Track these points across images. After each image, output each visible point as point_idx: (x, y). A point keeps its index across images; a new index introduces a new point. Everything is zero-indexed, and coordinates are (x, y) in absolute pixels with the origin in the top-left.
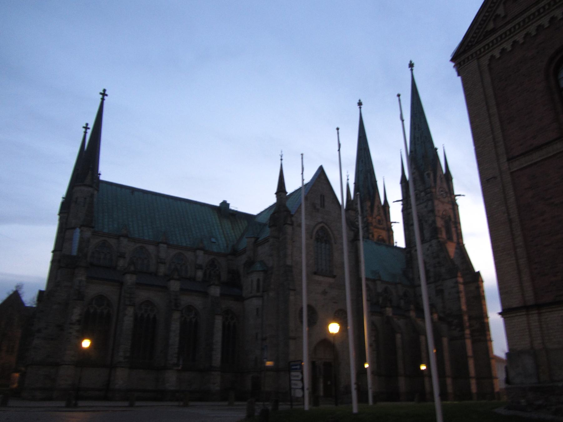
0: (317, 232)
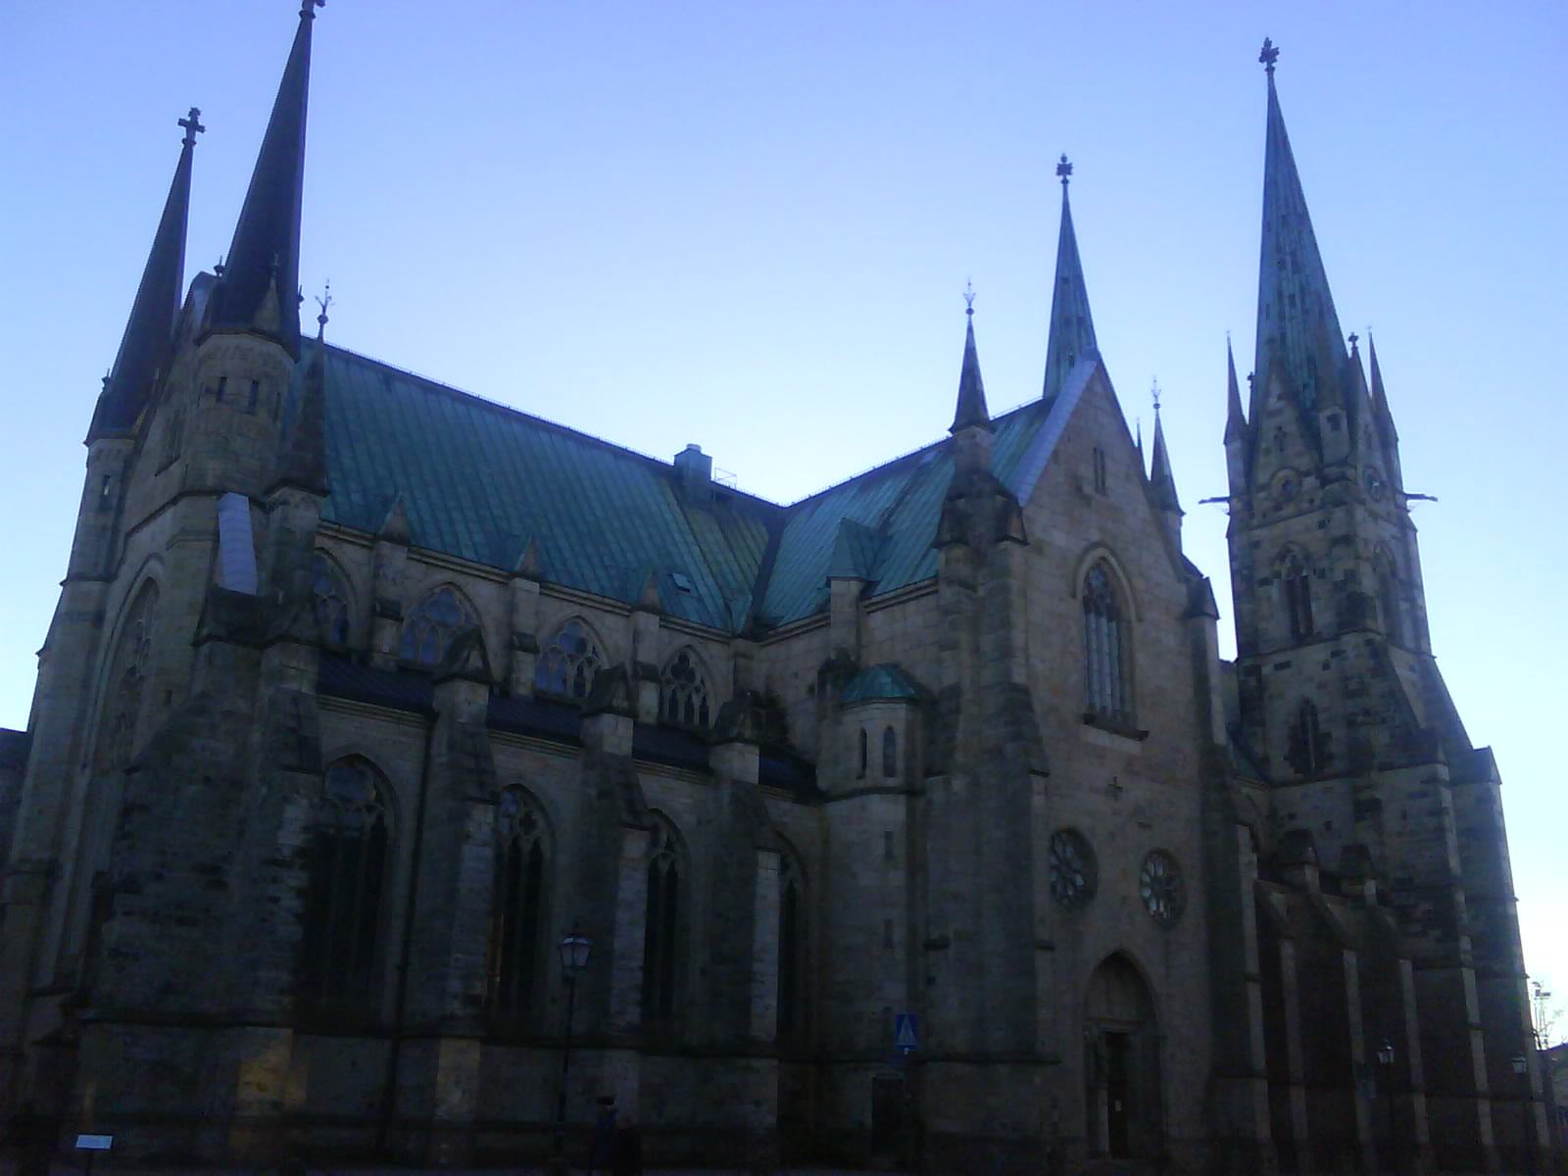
0: (1087, 578)
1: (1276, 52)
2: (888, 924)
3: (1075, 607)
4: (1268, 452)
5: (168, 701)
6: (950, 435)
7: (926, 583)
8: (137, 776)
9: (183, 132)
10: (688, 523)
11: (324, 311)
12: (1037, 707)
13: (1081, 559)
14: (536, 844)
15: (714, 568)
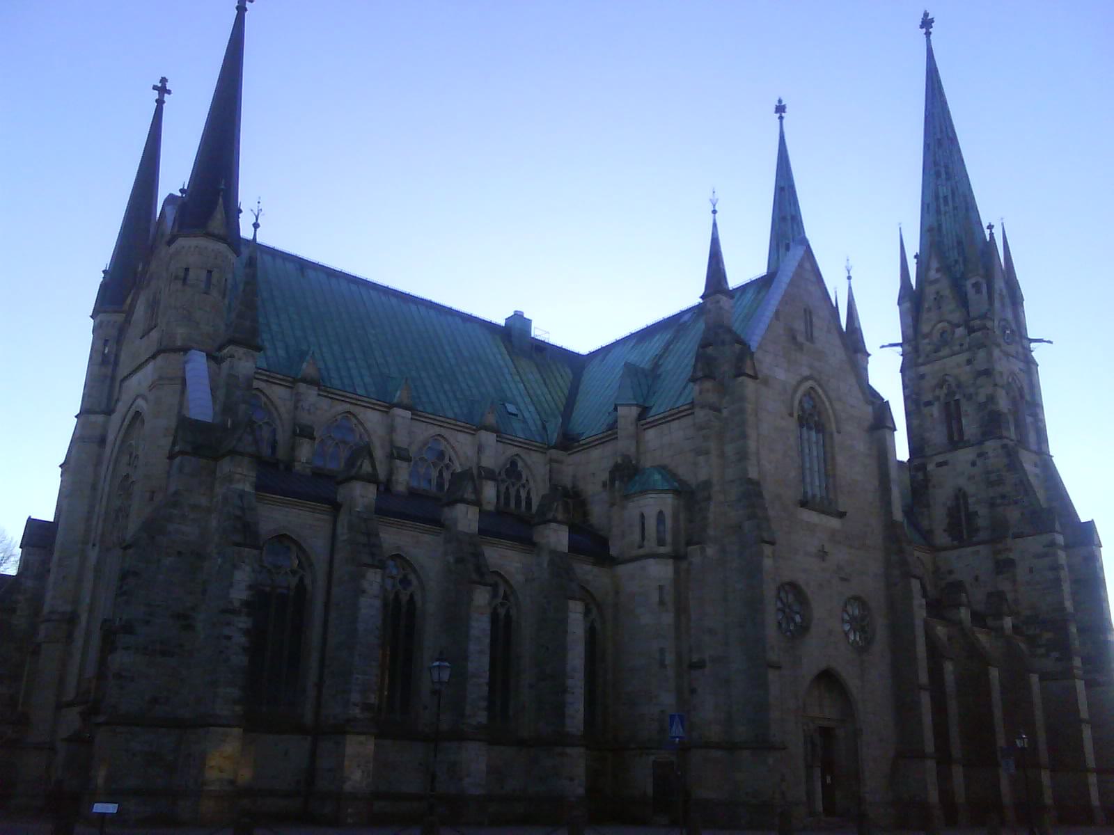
0: (801, 402)
1: (932, 21)
2: (662, 651)
3: (792, 424)
4: (929, 309)
5: (152, 499)
6: (701, 301)
7: (685, 407)
8: (130, 551)
9: (156, 94)
10: (516, 368)
11: (257, 219)
12: (766, 495)
13: (795, 391)
14: (412, 596)
15: (535, 399)
